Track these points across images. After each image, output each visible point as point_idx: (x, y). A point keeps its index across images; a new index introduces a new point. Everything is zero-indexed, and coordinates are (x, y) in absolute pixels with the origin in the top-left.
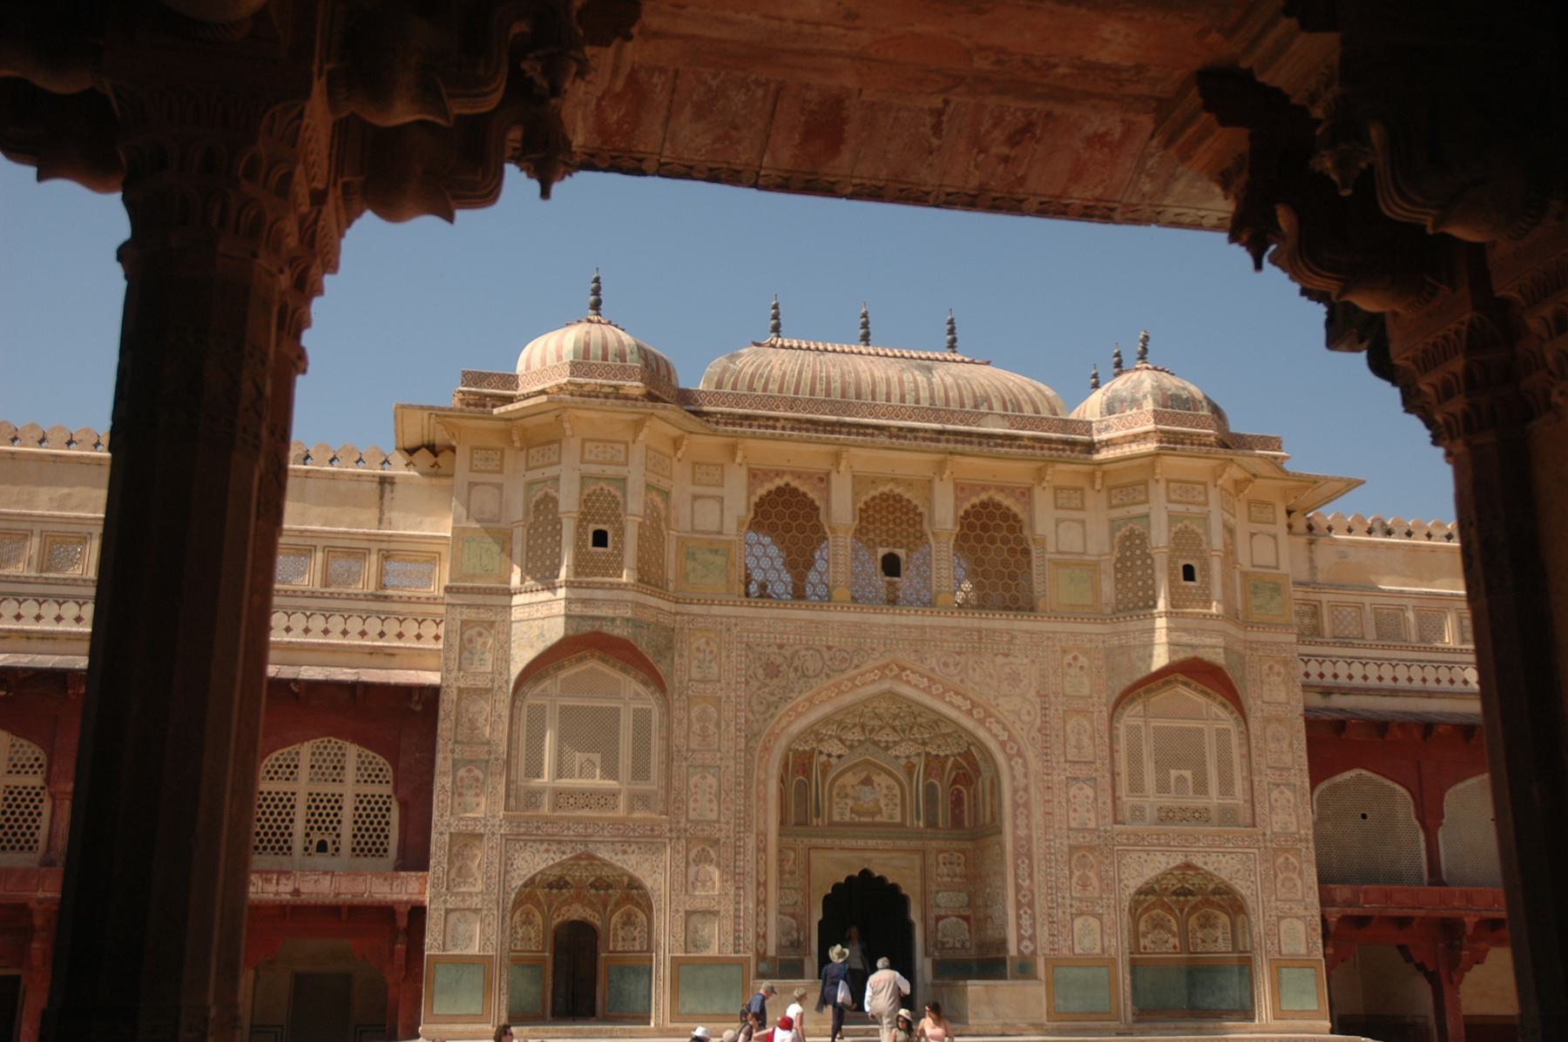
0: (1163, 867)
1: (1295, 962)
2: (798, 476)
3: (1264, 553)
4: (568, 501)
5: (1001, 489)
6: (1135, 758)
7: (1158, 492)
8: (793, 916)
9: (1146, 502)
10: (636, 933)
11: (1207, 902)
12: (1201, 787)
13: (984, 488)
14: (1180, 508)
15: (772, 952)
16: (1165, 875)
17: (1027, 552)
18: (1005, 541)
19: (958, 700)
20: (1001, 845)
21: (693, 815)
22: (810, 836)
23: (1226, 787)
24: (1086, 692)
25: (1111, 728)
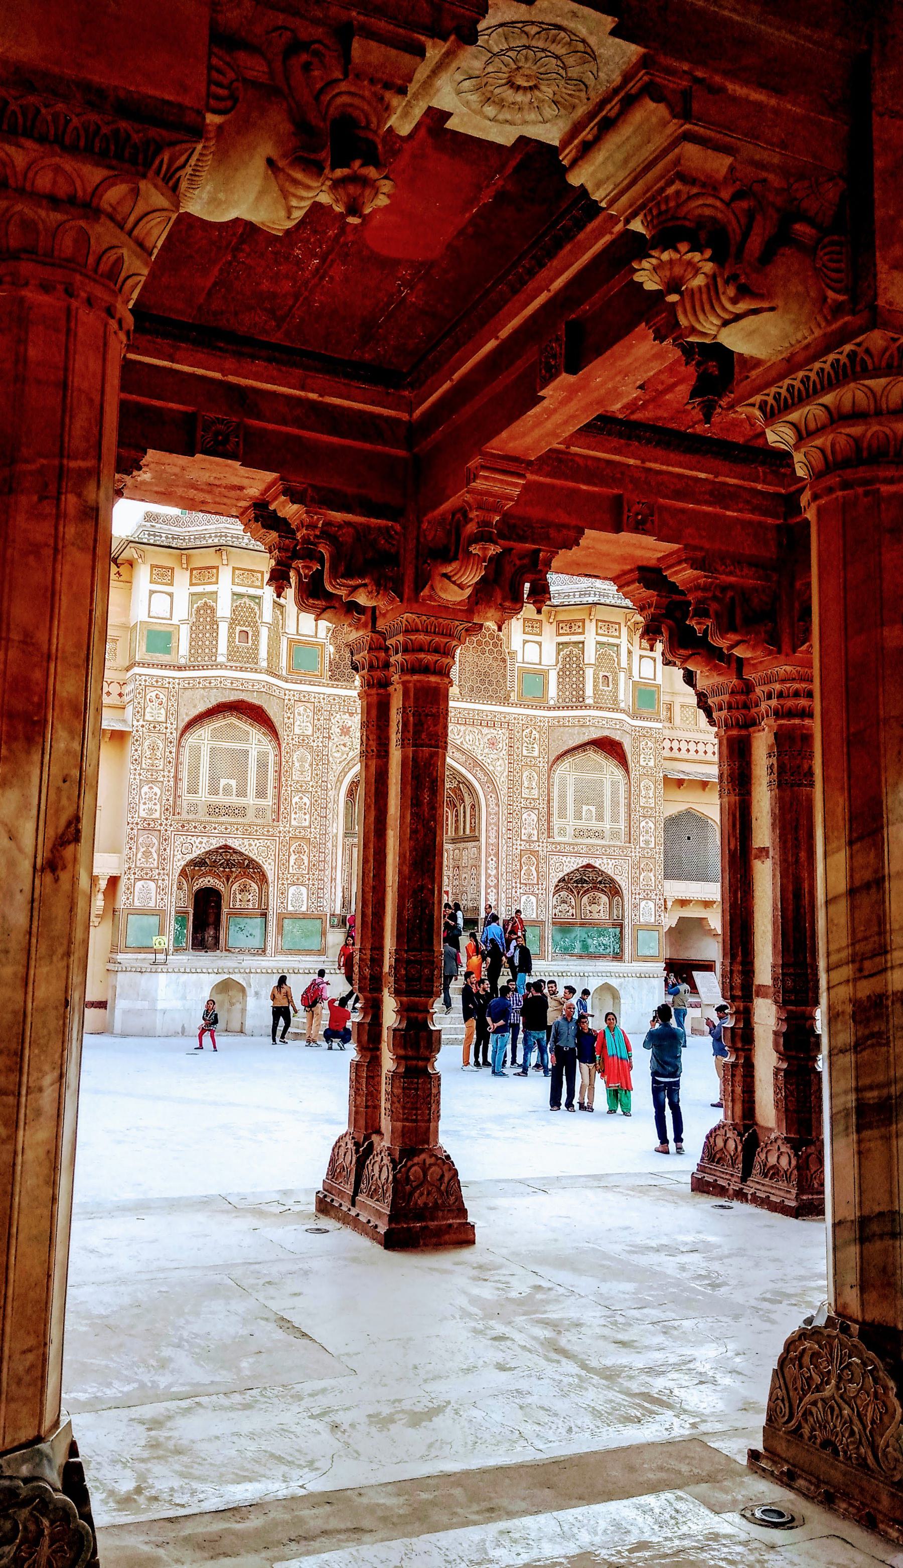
1: (649, 928)
4: (224, 608)
6: (563, 797)
7: (591, 627)
9: (583, 633)
10: (250, 897)
11: (595, 888)
12: (600, 818)
14: (604, 639)
17: (504, 661)
18: (491, 652)
20: (479, 848)
21: (294, 823)
23: (615, 819)
24: (536, 754)
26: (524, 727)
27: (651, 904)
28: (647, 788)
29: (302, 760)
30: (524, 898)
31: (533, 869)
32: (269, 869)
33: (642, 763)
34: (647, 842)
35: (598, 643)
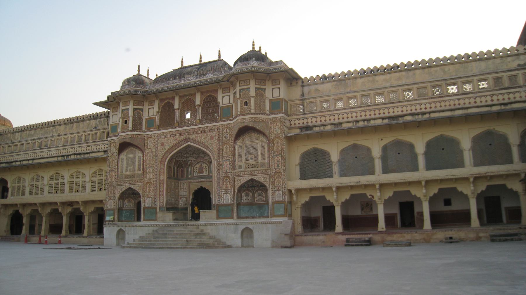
0: (246, 180)
2: (169, 99)
3: (276, 93)
5: (211, 91)
6: (240, 153)
7: (238, 84)
8: (186, 198)
12: (256, 158)
13: (207, 92)
14: (243, 87)
15: (165, 206)
16: (247, 182)
17: (218, 106)
19: (201, 145)
22: (189, 179)
23: (263, 158)
25: (234, 147)
26: (223, 129)
27: (281, 192)
28: (278, 143)
29: (150, 156)
30: (225, 195)
31: (228, 183)
32: (141, 193)
33: (275, 132)
34: (278, 166)
35: (240, 90)
